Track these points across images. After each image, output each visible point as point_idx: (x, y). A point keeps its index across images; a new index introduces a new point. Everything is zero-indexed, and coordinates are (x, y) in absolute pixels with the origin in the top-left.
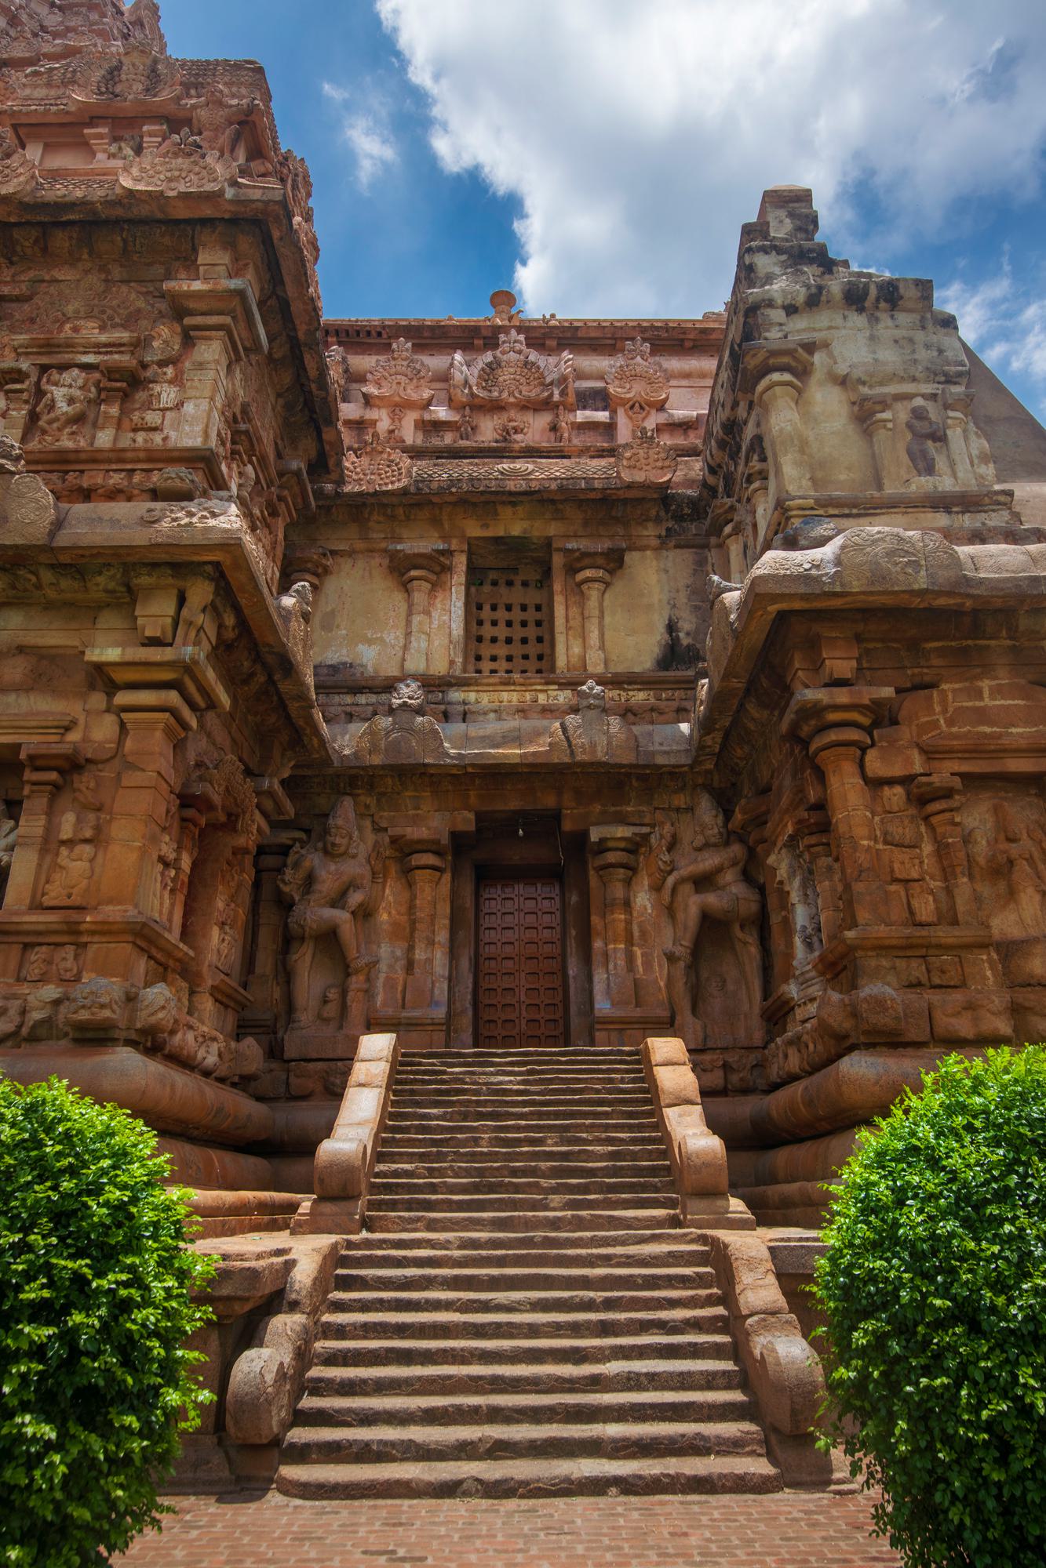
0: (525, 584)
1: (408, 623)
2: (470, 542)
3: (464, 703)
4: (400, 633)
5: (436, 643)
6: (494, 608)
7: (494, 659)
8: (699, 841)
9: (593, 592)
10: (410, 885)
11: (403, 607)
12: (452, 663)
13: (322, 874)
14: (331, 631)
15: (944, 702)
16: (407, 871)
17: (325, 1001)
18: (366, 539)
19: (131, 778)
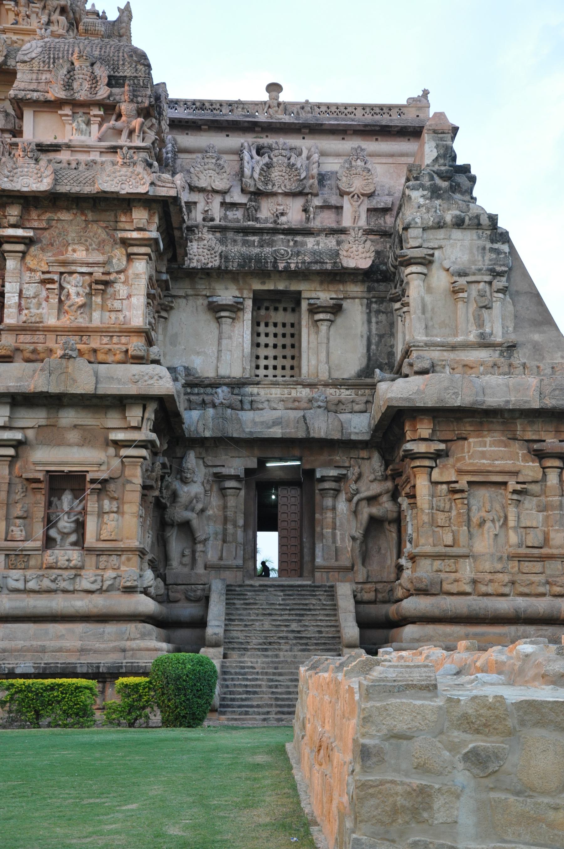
0: (285, 309)
1: (219, 344)
2: (255, 292)
3: (252, 395)
4: (215, 349)
5: (235, 356)
6: (267, 325)
7: (266, 358)
8: (372, 477)
9: (323, 327)
10: (224, 496)
11: (216, 332)
12: (244, 369)
13: (181, 493)
14: (176, 346)
15: (469, 447)
16: (223, 490)
17: (183, 555)
18: (193, 288)
19: (129, 487)
